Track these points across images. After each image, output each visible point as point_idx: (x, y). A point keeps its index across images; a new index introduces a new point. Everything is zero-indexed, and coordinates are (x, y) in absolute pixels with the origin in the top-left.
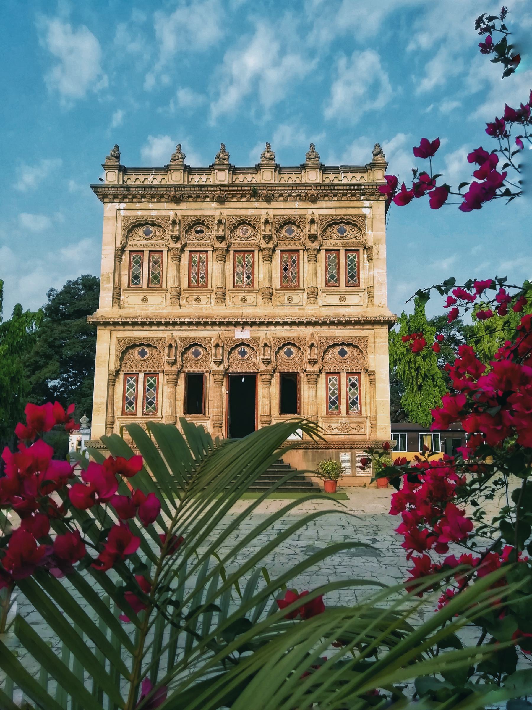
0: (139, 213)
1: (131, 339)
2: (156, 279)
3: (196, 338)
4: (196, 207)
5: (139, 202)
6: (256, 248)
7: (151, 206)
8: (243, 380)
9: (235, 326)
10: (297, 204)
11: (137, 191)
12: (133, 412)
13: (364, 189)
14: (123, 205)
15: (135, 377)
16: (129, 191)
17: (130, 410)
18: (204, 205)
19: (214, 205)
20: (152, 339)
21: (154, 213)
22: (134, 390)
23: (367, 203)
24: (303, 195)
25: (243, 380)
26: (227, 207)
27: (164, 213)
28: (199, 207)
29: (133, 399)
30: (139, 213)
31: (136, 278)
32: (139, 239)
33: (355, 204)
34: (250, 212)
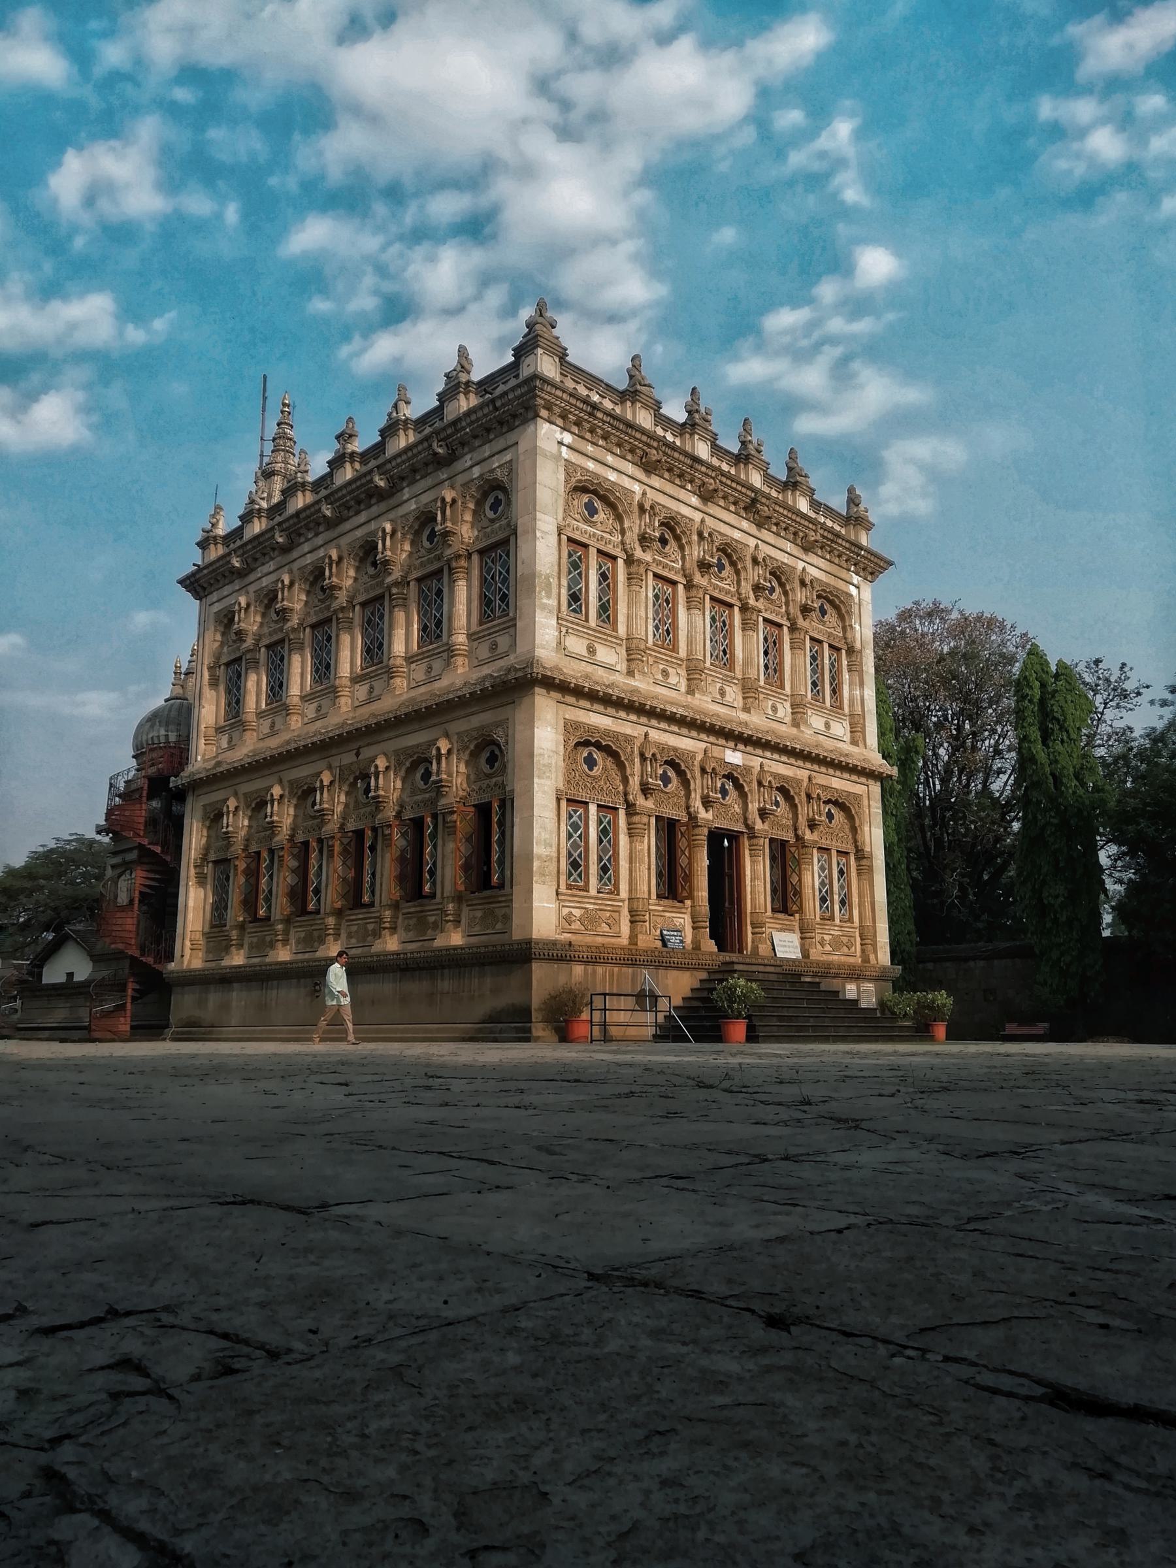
0: (591, 465)
1: (592, 729)
2: (606, 610)
3: (675, 749)
4: (671, 493)
5: (593, 443)
6: (738, 603)
7: (610, 459)
8: (726, 843)
9: (727, 740)
10: (789, 546)
11: (604, 422)
12: (582, 884)
13: (863, 556)
14: (568, 438)
15: (581, 811)
16: (591, 414)
17: (575, 880)
18: (682, 494)
19: (694, 500)
20: (616, 736)
21: (612, 476)
22: (580, 836)
23: (856, 579)
24: (801, 534)
25: (726, 843)
26: (711, 512)
27: (627, 483)
28: (675, 495)
29: (580, 855)
30: (591, 465)
31: (574, 597)
32: (577, 516)
33: (843, 574)
34: (737, 535)
